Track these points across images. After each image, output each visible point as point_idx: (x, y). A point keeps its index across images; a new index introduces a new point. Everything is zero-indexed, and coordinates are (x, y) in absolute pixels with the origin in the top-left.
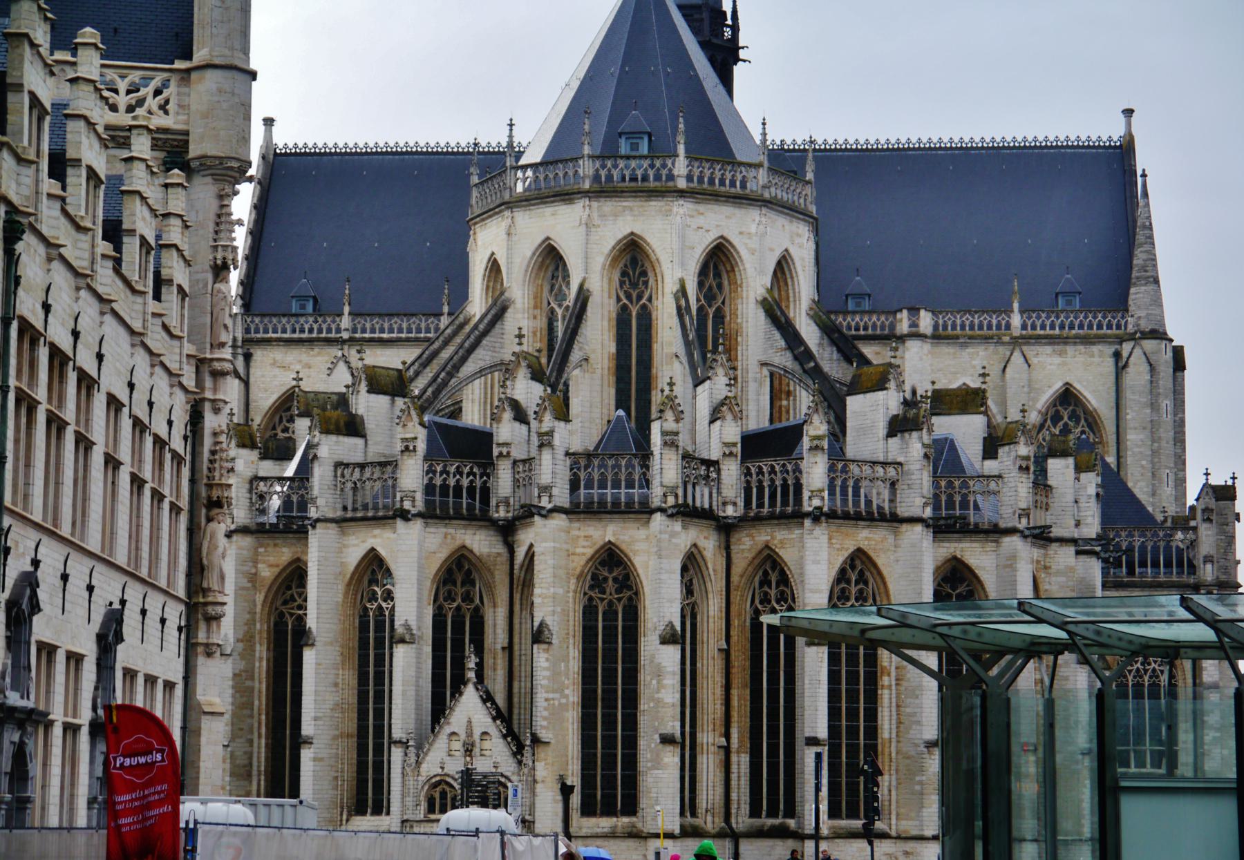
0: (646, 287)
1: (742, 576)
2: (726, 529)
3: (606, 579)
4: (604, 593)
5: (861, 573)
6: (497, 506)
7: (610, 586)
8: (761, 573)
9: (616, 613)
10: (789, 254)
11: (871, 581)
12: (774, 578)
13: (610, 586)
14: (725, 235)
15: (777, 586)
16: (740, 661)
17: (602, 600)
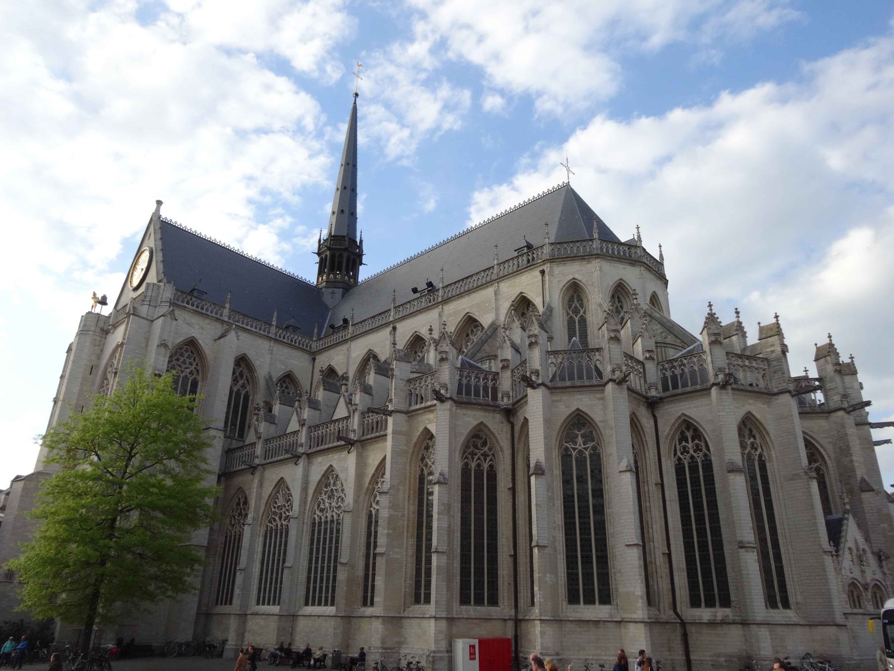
0: (582, 308)
1: (666, 438)
2: (652, 405)
3: (577, 435)
4: (575, 443)
5: (751, 431)
6: (502, 397)
7: (580, 440)
8: (679, 432)
9: (585, 457)
10: (656, 294)
11: (758, 437)
12: (689, 435)
13: (580, 440)
14: (624, 279)
15: (693, 440)
16: (672, 493)
17: (574, 449)
